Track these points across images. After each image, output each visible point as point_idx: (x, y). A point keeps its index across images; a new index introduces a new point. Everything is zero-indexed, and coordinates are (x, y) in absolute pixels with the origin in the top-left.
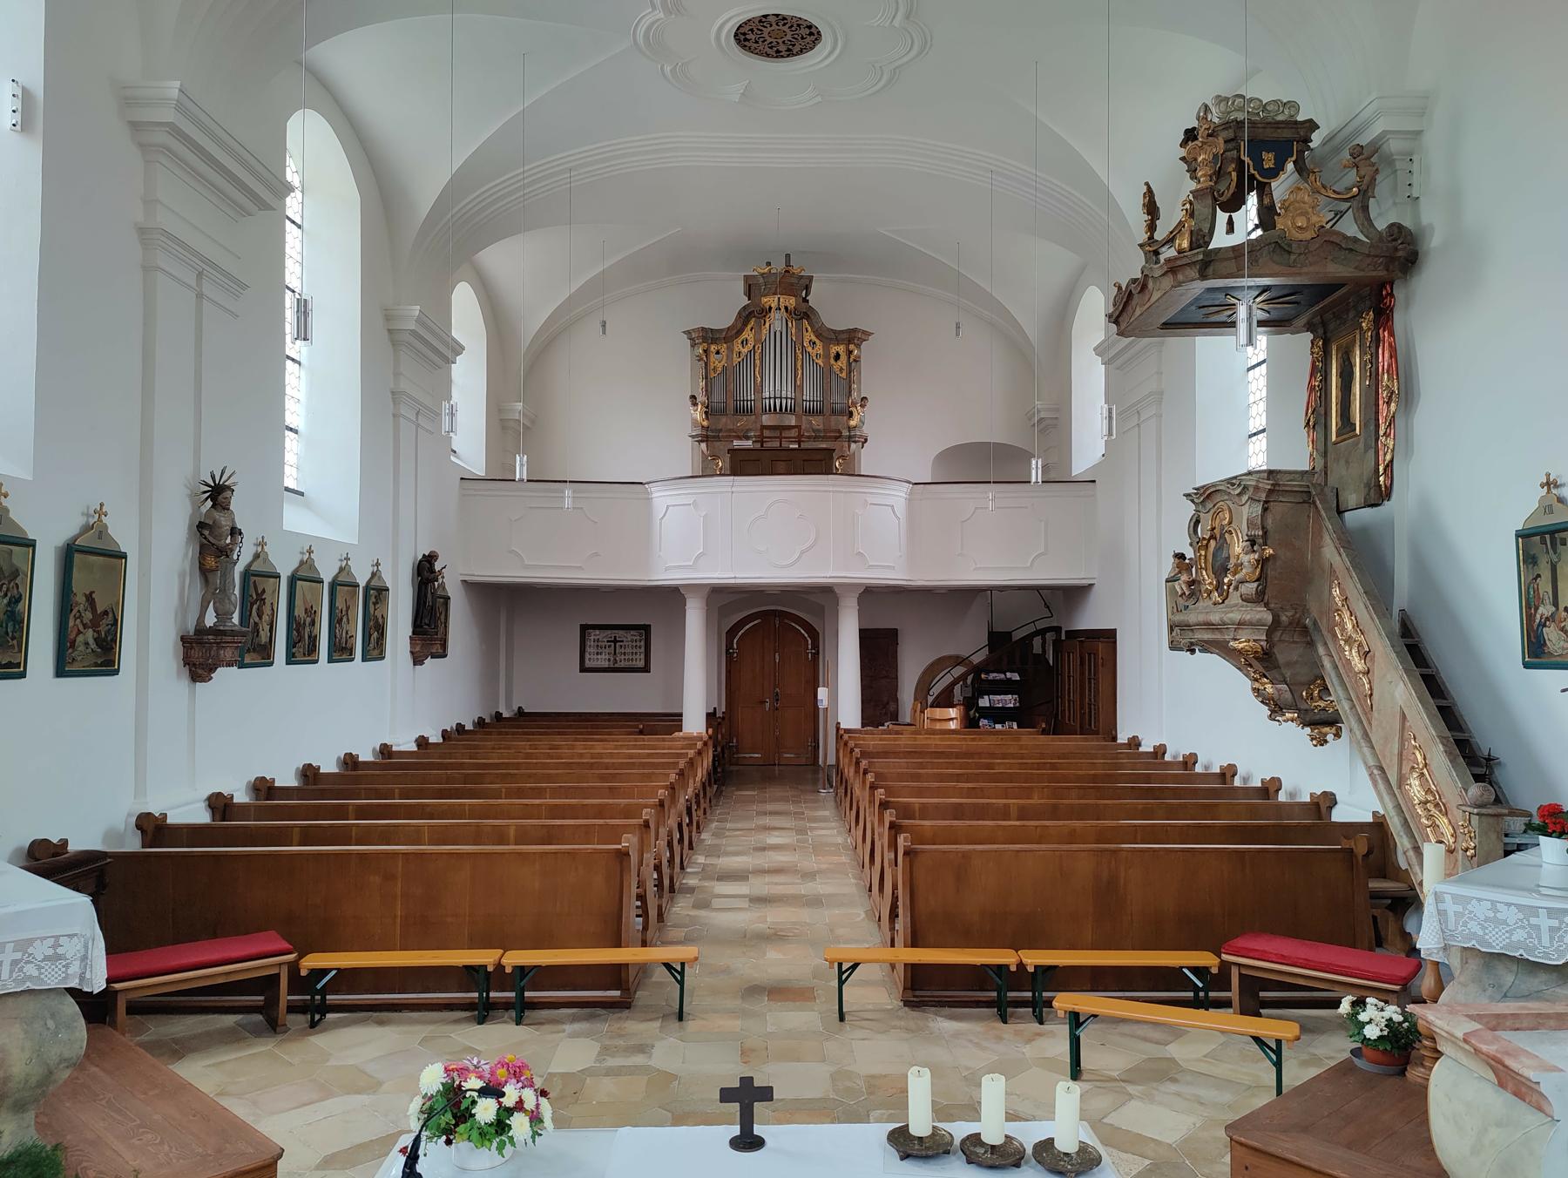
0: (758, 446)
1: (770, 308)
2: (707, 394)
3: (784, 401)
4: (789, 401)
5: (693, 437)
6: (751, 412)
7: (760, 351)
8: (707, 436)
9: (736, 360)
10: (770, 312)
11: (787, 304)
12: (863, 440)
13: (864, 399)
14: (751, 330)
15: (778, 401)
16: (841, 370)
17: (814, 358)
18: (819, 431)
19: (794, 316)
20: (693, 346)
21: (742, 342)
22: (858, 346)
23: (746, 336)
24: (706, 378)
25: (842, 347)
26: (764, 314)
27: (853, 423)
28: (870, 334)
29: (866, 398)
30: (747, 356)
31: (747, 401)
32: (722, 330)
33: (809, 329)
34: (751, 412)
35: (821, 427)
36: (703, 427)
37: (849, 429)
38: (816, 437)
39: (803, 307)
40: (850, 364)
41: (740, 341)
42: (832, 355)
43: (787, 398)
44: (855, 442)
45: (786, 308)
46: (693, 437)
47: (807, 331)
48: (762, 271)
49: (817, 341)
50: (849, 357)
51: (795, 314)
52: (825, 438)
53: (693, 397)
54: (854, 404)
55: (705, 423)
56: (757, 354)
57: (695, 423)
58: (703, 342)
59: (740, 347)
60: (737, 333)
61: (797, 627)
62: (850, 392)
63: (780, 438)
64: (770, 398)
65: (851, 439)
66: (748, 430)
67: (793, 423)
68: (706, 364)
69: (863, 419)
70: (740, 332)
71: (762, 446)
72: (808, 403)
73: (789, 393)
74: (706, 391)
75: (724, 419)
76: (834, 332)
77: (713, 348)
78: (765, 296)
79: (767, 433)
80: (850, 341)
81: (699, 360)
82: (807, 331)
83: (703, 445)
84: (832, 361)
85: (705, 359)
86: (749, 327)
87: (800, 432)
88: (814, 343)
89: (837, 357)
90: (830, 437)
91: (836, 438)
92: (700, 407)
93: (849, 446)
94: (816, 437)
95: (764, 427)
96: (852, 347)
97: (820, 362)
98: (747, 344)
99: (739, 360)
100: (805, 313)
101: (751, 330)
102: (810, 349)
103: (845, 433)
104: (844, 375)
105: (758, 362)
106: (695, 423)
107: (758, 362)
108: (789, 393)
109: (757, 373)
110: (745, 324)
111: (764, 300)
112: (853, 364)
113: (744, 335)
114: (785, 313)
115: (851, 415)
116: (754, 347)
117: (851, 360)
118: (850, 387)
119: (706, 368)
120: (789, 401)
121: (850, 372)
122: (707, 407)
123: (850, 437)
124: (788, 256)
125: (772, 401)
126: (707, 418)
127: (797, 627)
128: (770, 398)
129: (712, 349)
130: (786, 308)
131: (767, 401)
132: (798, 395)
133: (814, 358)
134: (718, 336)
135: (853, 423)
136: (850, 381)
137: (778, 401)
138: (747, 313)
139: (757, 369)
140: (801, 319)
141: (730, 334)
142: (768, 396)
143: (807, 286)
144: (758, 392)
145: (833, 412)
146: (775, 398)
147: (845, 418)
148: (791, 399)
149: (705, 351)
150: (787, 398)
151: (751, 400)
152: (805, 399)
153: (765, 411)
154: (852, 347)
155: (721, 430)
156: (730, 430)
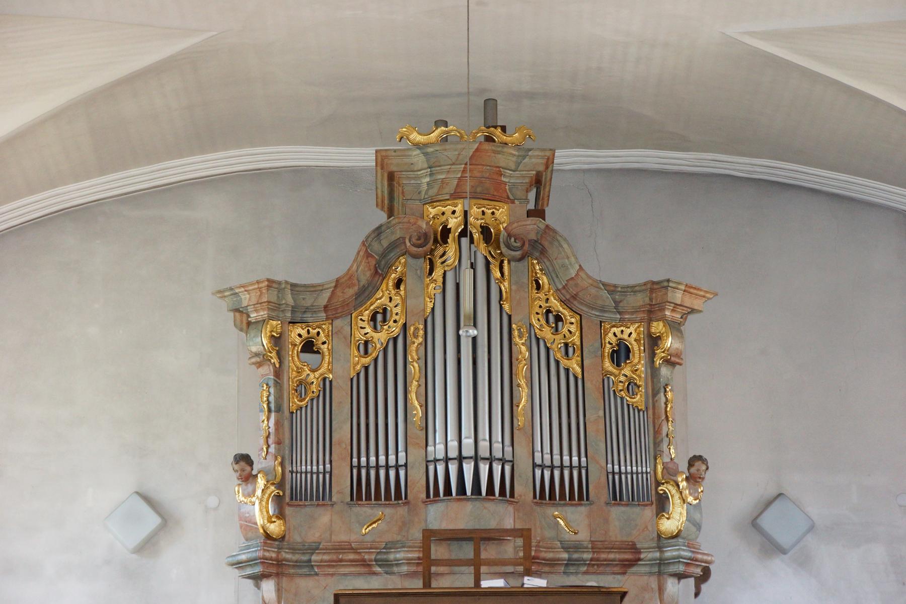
0: (416, 584)
1: (446, 231)
3: (484, 469)
7: (420, 340)
8: (279, 563)
10: (445, 241)
11: (489, 219)
12: (698, 571)
13: (695, 460)
16: (631, 386)
18: (577, 547)
19: (504, 249)
21: (373, 318)
23: (385, 300)
24: (279, 409)
26: (430, 245)
27: (669, 525)
29: (698, 458)
30: (385, 350)
34: (398, 496)
35: (584, 536)
36: (268, 536)
37: (662, 540)
38: (570, 563)
39: (532, 226)
40: (654, 372)
41: (367, 315)
42: (608, 349)
43: (491, 460)
44: (680, 576)
45: (485, 231)
46: (239, 565)
51: (509, 247)
52: (596, 565)
53: (244, 459)
54: (671, 472)
55: (275, 528)
57: (247, 525)
58: (271, 318)
59: (368, 330)
60: (358, 295)
62: (657, 444)
63: (476, 563)
65: (661, 568)
66: (390, 546)
67: (509, 524)
68: (278, 373)
69: (697, 516)
70: (365, 293)
71: (427, 584)
72: (547, 474)
73: (497, 446)
74: (279, 443)
75: (324, 517)
76: (612, 289)
78: (432, 202)
79: (438, 551)
80: (652, 312)
81: (259, 365)
83: (269, 587)
84: (608, 365)
85: (275, 360)
87: (527, 546)
88: (558, 318)
89: (621, 353)
90: (609, 563)
91: (627, 565)
93: (661, 589)
94: (570, 563)
95: (430, 536)
96: (658, 327)
98: (384, 320)
99: (366, 361)
100: (534, 244)
105: (415, 368)
108: (497, 446)
109: (412, 396)
110: (380, 272)
111: (432, 211)
112: (665, 371)
114: (483, 245)
115: (662, 504)
117: (658, 362)
118: (657, 432)
119: (278, 384)
120: (497, 468)
121: (655, 394)
122: (280, 485)
124: (490, 105)
125: (453, 468)
126: (281, 515)
128: (447, 460)
130: (485, 231)
131: (441, 468)
132: (522, 452)
134: (308, 303)
135: (669, 525)
137: (468, 468)
138: (385, 243)
139: (413, 386)
141: (340, 296)
142: (441, 455)
145: (616, 497)
148: (503, 461)
150: (491, 460)
152: (538, 461)
153: (432, 494)
154: (658, 327)
155: (314, 548)
156: (348, 547)
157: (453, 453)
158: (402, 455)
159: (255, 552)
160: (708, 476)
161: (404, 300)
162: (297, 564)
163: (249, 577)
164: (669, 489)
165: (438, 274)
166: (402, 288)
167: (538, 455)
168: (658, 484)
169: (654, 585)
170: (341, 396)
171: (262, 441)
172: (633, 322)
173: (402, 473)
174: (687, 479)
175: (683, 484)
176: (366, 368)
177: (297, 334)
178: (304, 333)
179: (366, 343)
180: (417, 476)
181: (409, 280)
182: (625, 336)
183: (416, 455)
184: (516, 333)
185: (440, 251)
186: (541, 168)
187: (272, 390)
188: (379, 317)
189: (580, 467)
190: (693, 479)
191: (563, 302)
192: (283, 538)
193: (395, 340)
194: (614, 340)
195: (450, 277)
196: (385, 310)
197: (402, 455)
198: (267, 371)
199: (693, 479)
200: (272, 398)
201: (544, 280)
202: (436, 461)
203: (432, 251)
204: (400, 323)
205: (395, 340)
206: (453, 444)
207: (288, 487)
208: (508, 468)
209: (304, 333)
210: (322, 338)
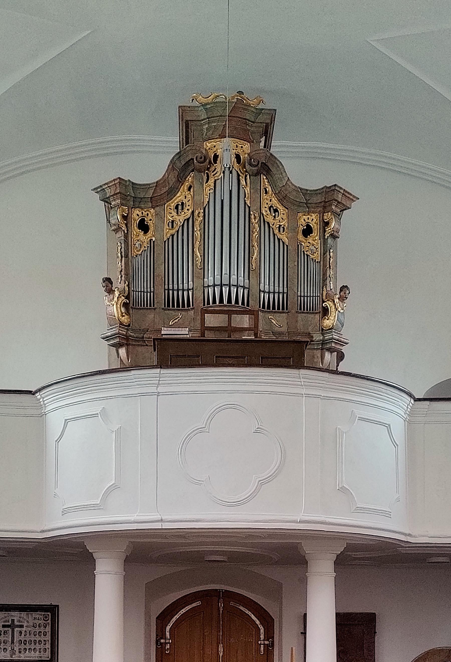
2: (126, 279)
3: (234, 290)
4: (241, 291)
5: (107, 338)
6: (189, 305)
8: (127, 338)
9: (167, 232)
11: (240, 151)
13: (344, 288)
14: (189, 189)
15: (225, 290)
17: (276, 231)
18: (281, 334)
20: (109, 209)
21: (177, 207)
22: (338, 216)
23: (182, 198)
24: (127, 256)
25: (314, 216)
27: (327, 323)
28: (354, 198)
30: (183, 225)
31: (183, 290)
32: (146, 187)
33: (269, 189)
34: (189, 305)
36: (121, 324)
37: (323, 331)
40: (325, 241)
41: (173, 205)
43: (237, 286)
46: (107, 338)
47: (266, 193)
48: (204, 101)
49: (280, 208)
50: (325, 231)
55: (125, 319)
56: (197, 223)
61: (247, 612)
62: (325, 280)
64: (214, 286)
68: (126, 236)
69: (341, 318)
70: (172, 192)
72: (267, 296)
73: (241, 279)
74: (127, 274)
77: (136, 214)
82: (266, 193)
86: (187, 184)
88: (276, 211)
89: (308, 231)
92: (117, 293)
96: (328, 216)
97: (284, 237)
98: (182, 209)
101: (189, 189)
102: (270, 219)
103: (317, 337)
104: (317, 256)
106: (111, 320)
107: (198, 234)
108: (241, 279)
109: (196, 250)
110: (180, 180)
111: (208, 145)
112: (330, 240)
113: (179, 197)
115: (325, 311)
116: (193, 212)
117: (327, 235)
119: (126, 241)
120: (241, 291)
122: (127, 297)
123: (324, 342)
125: (217, 290)
126: (128, 313)
127: (247, 612)
128: (214, 286)
129: (134, 215)
131: (211, 290)
133: (276, 231)
135: (327, 323)
136: (325, 266)
137: (225, 290)
140: (258, 174)
142: (211, 283)
143: (267, 126)
144: (198, 277)
146: (221, 286)
147: (317, 316)
148: (244, 287)
149: (125, 218)
150: (237, 286)
151: (188, 290)
152: (262, 289)
154: (328, 216)
157: (218, 282)
158: (191, 283)
159: (115, 330)
160: (349, 296)
161: (193, 198)
162: (137, 339)
163: (113, 345)
164: (328, 304)
165: (211, 181)
166: (192, 190)
167: (262, 285)
168: (323, 302)
169: (319, 355)
170: (159, 250)
171: (118, 273)
172: (313, 212)
173: (190, 293)
174: (339, 298)
175: (336, 300)
176: (173, 236)
177: (136, 214)
178: (140, 214)
179: (173, 222)
180: (199, 295)
181: (196, 186)
182: (309, 221)
183: (198, 283)
184: (252, 217)
185: (213, 168)
186: (268, 121)
187: (123, 245)
188: (180, 207)
189: (283, 293)
190: (342, 299)
191: (280, 201)
192: (129, 325)
193: (188, 220)
194: (304, 223)
195: (218, 182)
196: (183, 204)
197: (191, 283)
198: (120, 235)
199: (342, 299)
200: (123, 250)
201: (269, 189)
202: (209, 286)
203: (208, 169)
204: (190, 211)
205: (188, 220)
206: (218, 277)
207: (131, 299)
208: (246, 291)
209: (140, 214)
210: (150, 217)
